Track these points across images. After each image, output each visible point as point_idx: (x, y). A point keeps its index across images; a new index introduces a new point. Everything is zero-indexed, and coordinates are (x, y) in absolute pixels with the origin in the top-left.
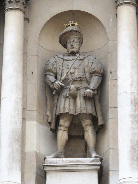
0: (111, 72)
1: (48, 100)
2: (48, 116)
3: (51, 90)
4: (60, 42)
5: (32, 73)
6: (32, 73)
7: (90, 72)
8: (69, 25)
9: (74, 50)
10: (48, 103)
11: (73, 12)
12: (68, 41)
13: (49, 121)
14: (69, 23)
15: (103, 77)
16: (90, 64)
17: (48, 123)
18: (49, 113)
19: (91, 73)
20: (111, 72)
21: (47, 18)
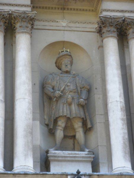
0: (96, 89)
1: (46, 107)
2: (45, 119)
3: (50, 99)
4: (56, 63)
5: (35, 84)
6: (35, 84)
7: (80, 87)
8: (64, 51)
9: (67, 69)
10: (46, 109)
11: (64, 42)
12: (63, 63)
13: (46, 123)
14: (63, 49)
15: (89, 91)
16: (80, 81)
17: (45, 125)
18: (45, 117)
19: (81, 88)
20: (96, 89)
21: (45, 45)
